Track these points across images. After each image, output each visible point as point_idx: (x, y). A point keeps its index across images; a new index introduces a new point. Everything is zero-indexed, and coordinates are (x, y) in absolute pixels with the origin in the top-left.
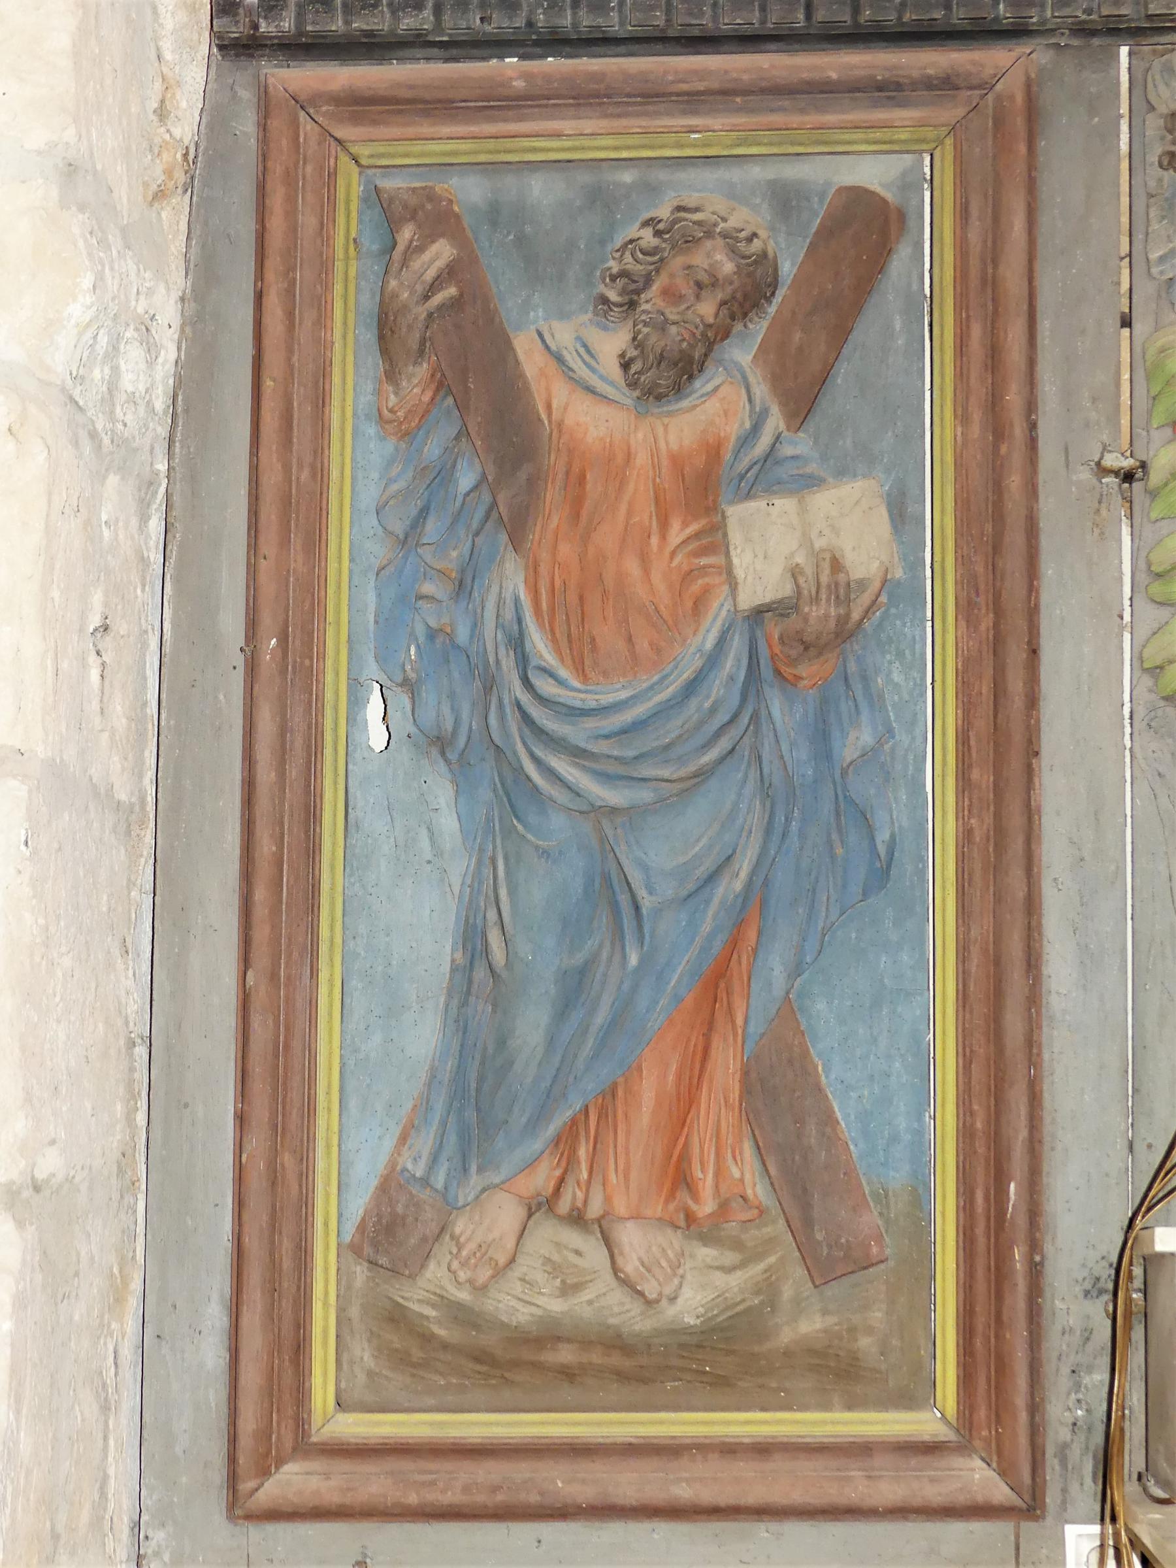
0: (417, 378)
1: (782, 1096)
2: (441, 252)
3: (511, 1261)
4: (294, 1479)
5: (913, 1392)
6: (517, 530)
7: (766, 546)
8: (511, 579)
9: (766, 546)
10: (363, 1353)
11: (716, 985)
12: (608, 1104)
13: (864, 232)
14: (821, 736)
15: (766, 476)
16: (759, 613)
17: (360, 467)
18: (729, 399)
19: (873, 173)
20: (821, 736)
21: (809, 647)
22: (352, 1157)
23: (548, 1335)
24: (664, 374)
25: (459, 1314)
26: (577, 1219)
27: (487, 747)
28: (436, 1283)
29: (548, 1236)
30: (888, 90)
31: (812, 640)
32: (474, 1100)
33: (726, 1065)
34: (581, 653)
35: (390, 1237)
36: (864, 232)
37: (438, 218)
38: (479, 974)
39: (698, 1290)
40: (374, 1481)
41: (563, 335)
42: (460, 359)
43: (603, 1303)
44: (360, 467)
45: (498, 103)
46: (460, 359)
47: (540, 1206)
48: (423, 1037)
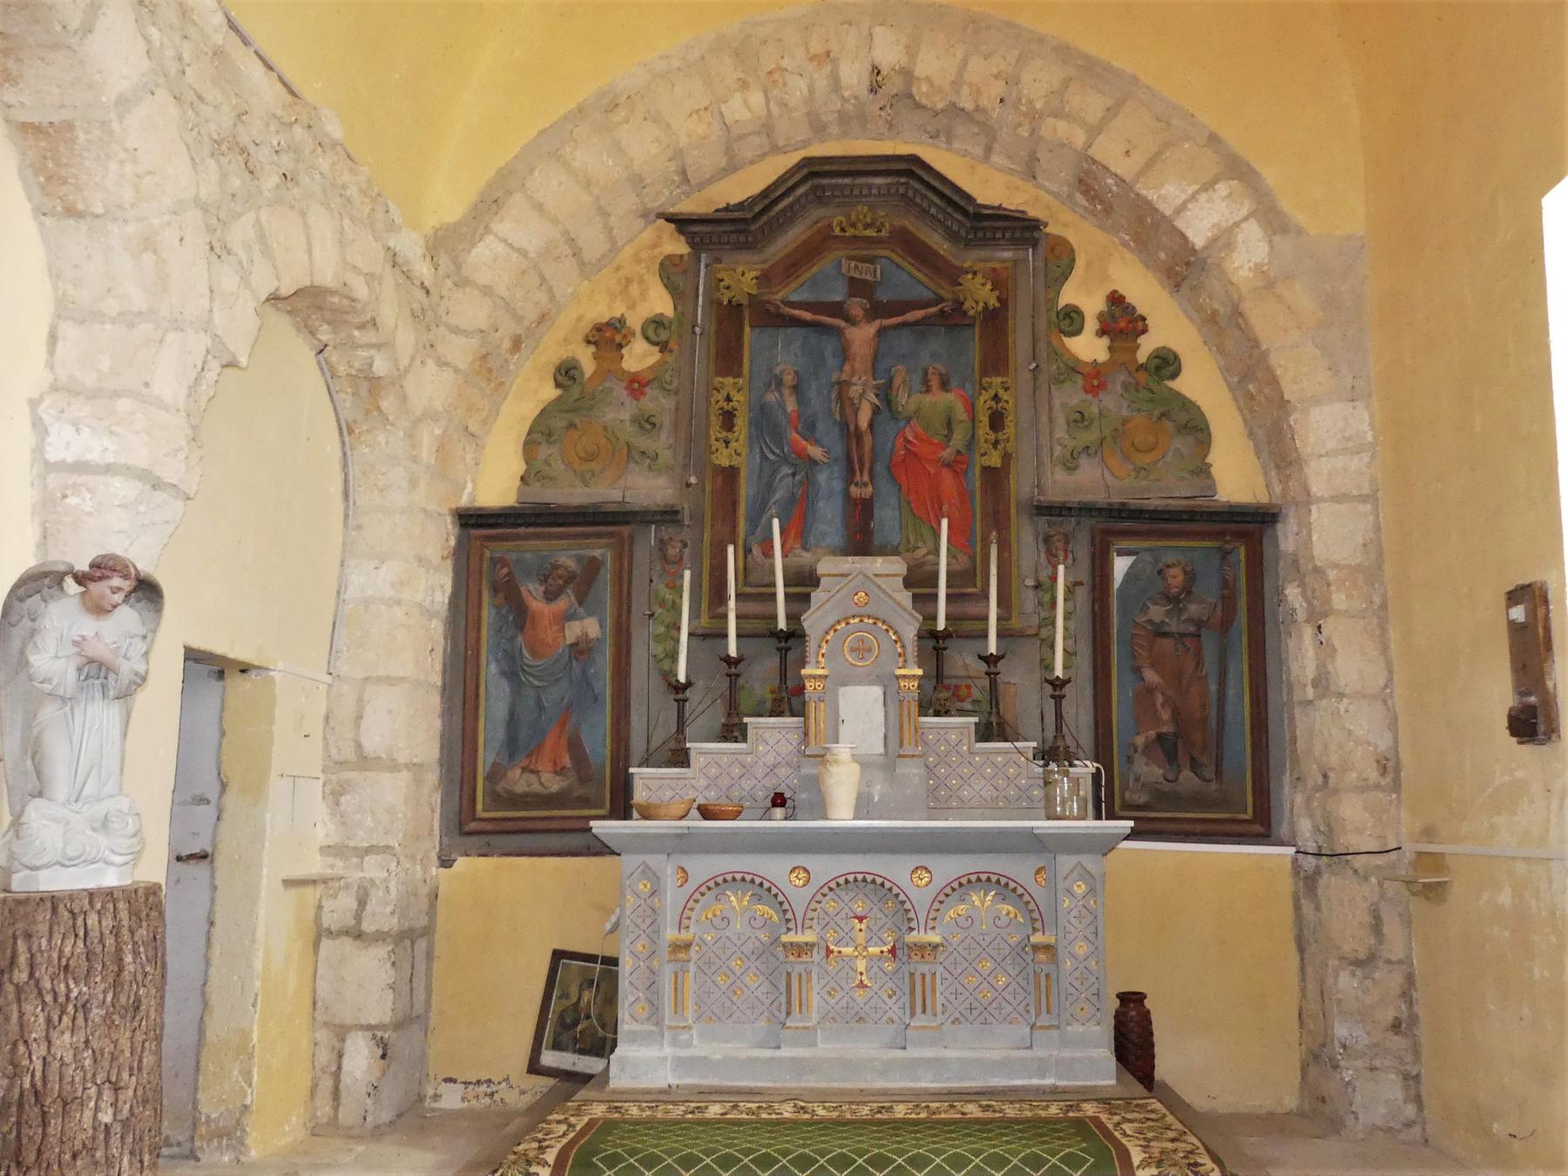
0: (501, 595)
1: (575, 746)
2: (505, 570)
3: (519, 781)
4: (473, 826)
5: (602, 806)
6: (521, 628)
7: (573, 631)
8: (520, 639)
9: (573, 631)
10: (488, 800)
11: (563, 724)
12: (540, 746)
13: (593, 566)
14: (584, 672)
15: (571, 617)
16: (572, 645)
17: (487, 614)
18: (564, 602)
19: (597, 553)
20: (584, 672)
21: (581, 652)
22: (485, 759)
23: (526, 795)
24: (550, 596)
25: (508, 792)
26: (532, 772)
27: (513, 672)
28: (501, 787)
29: (527, 775)
30: (600, 535)
31: (581, 650)
32: (512, 745)
33: (564, 741)
34: (534, 653)
35: (494, 776)
36: (593, 566)
37: (505, 564)
38: (512, 720)
39: (554, 784)
40: (489, 826)
41: (531, 587)
42: (509, 593)
43: (536, 788)
44: (487, 614)
45: (517, 537)
46: (509, 593)
47: (524, 770)
48: (500, 733)
